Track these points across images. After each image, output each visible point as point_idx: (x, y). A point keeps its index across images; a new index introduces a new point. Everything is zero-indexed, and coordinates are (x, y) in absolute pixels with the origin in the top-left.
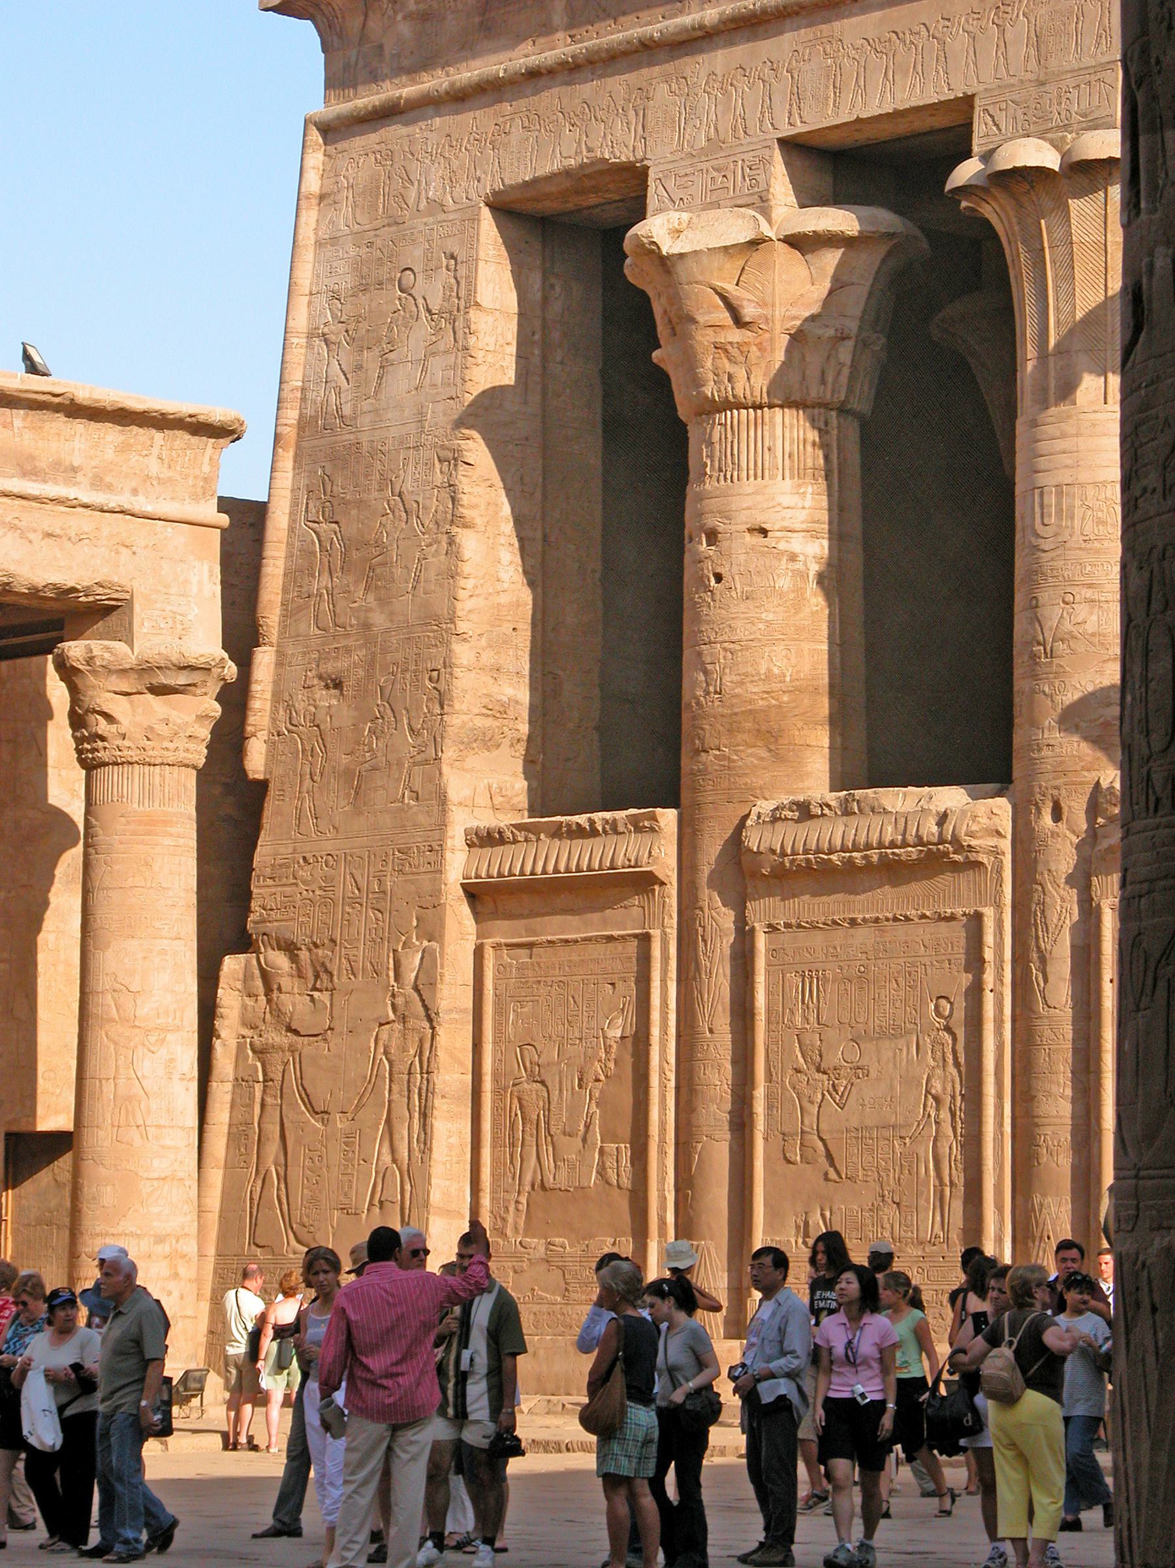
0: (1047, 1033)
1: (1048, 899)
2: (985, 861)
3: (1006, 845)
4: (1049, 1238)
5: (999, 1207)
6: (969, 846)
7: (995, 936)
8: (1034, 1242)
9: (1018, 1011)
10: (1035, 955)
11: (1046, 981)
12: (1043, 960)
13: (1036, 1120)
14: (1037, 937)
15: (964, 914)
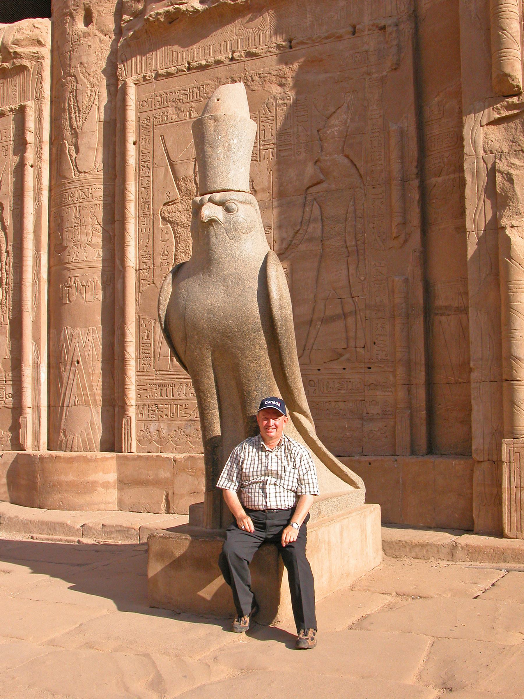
0: (78, 193)
1: (79, 87)
2: (28, 65)
3: (46, 51)
4: (78, 362)
5: (37, 340)
6: (15, 53)
7: (35, 122)
8: (65, 366)
9: (53, 183)
10: (68, 133)
11: (77, 151)
12: (76, 135)
13: (68, 266)
14: (70, 118)
15: (12, 110)
